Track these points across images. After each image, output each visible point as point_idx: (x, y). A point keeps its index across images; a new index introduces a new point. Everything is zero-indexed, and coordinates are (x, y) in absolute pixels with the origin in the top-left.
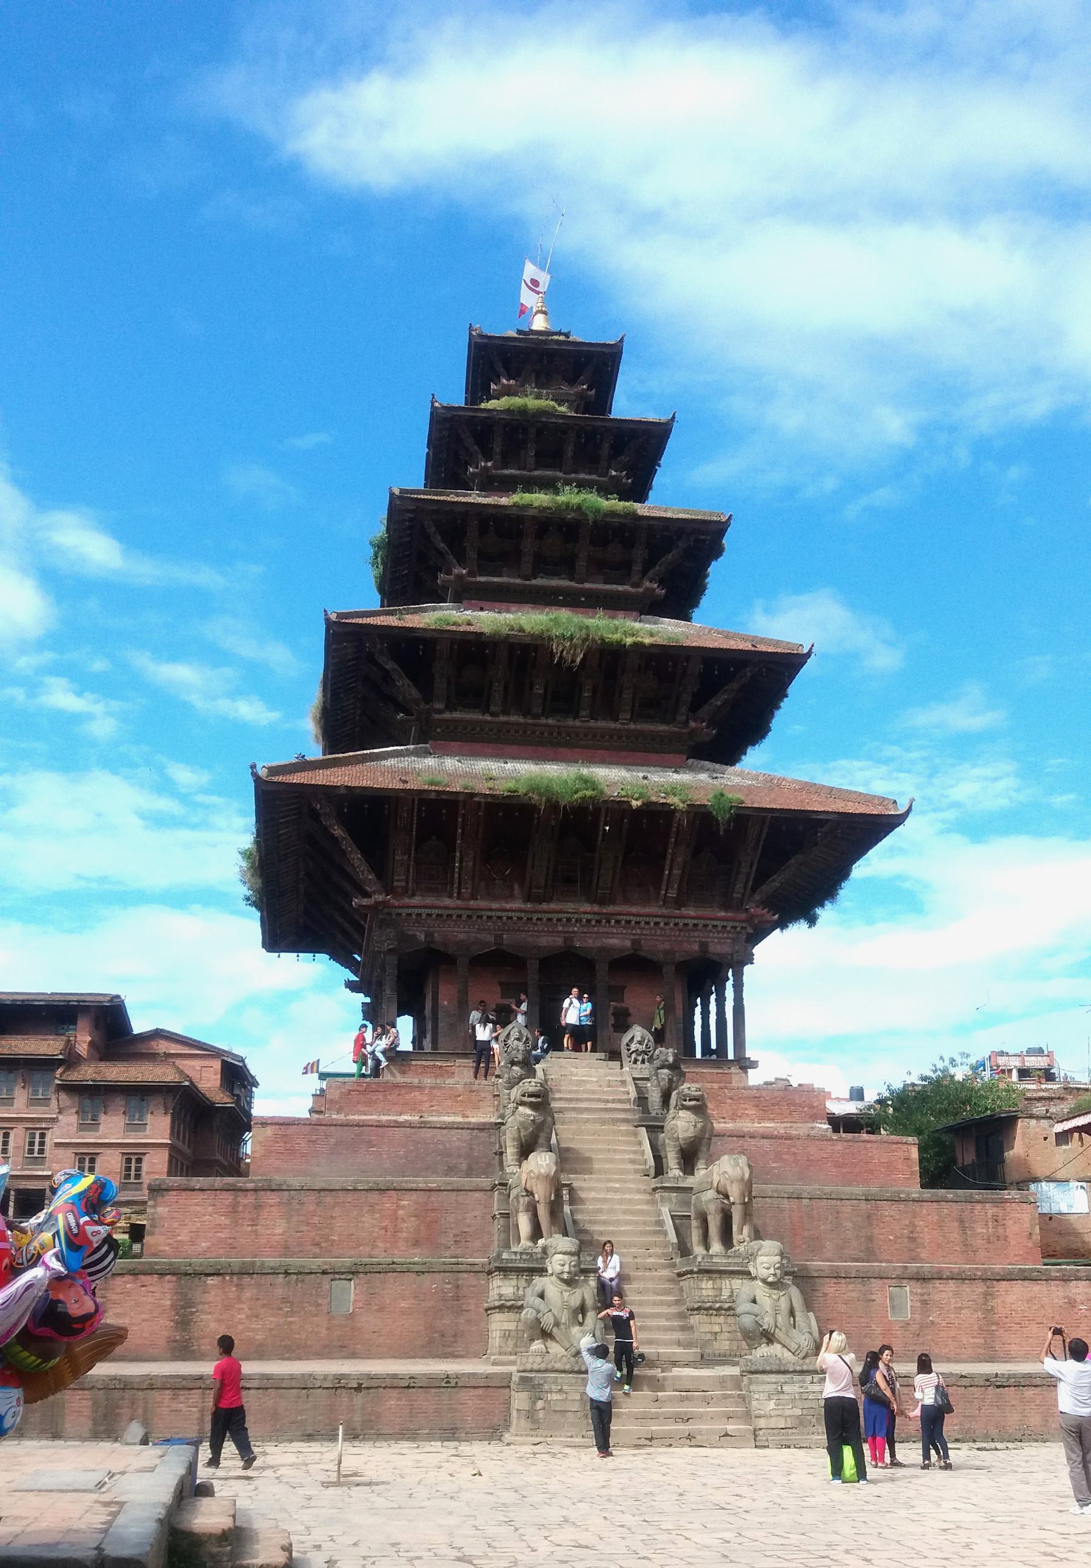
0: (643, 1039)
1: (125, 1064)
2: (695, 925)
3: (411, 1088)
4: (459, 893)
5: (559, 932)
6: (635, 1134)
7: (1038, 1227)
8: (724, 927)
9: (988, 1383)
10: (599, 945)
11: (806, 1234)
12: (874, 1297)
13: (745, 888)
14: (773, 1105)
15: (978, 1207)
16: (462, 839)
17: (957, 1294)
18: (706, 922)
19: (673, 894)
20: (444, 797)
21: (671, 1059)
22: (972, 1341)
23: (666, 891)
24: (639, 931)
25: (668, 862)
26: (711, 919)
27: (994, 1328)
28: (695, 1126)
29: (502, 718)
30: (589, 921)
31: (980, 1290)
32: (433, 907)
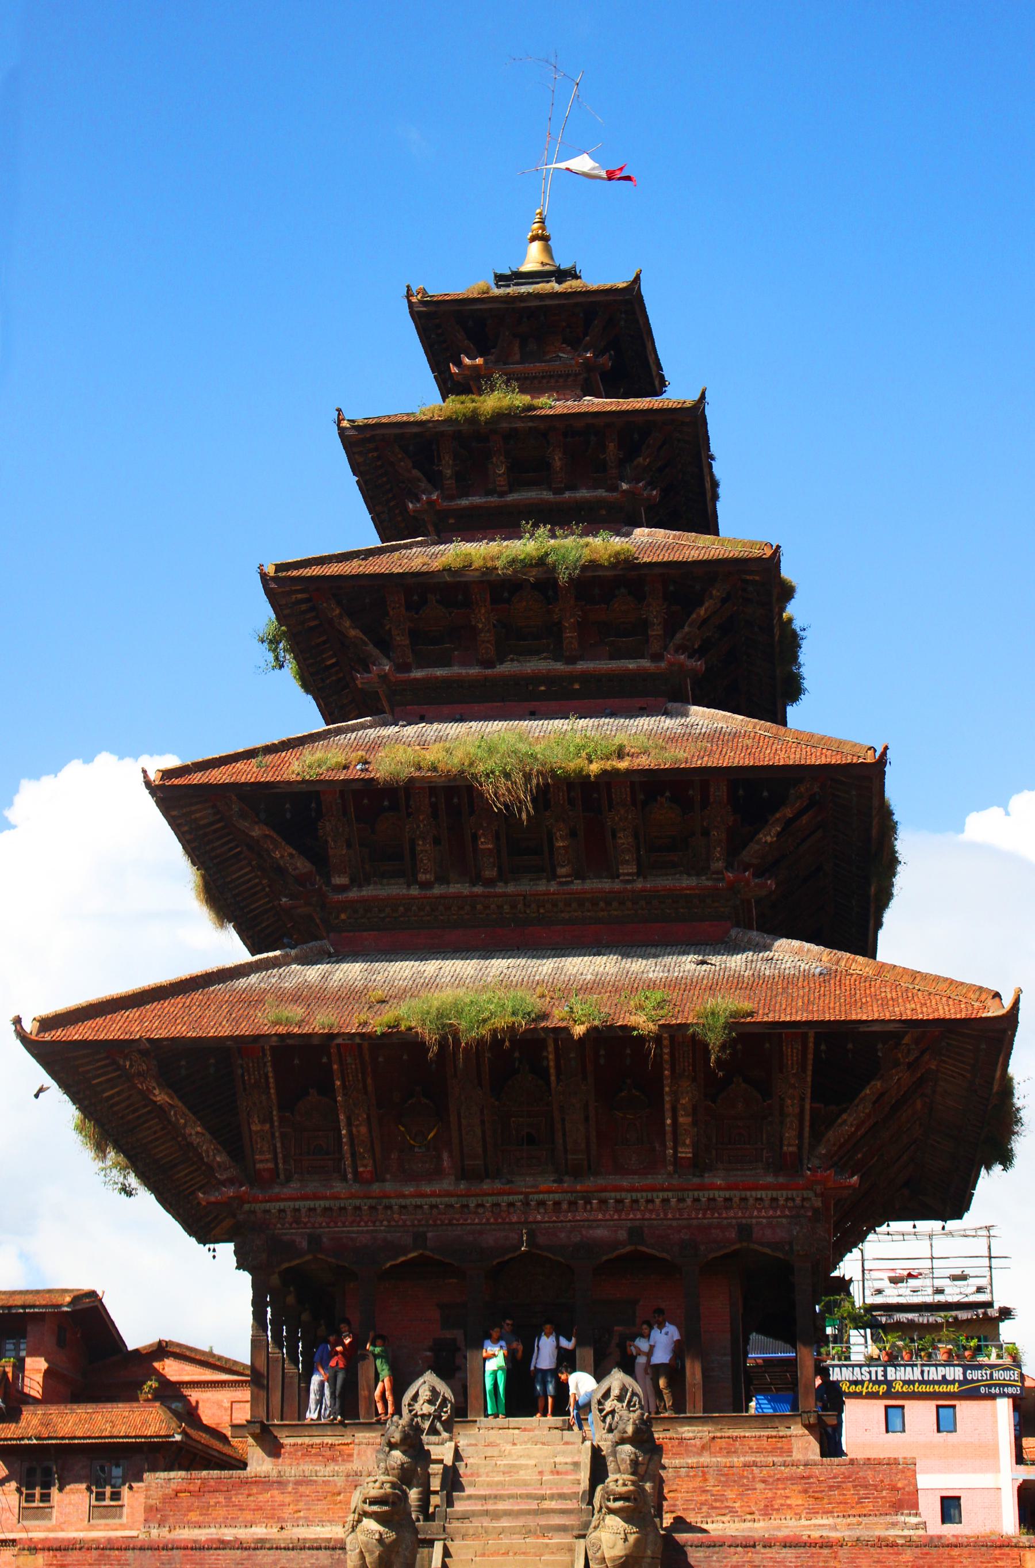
0: (624, 1389)
1: (90, 1408)
2: (726, 1200)
3: (263, 1483)
4: (356, 1173)
5: (511, 1223)
6: (571, 1550)
8: (774, 1200)
16: (344, 1095)
18: (743, 1194)
19: (686, 1152)
20: (290, 1042)
21: (630, 1429)
24: (639, 1216)
25: (667, 1106)
26: (750, 1189)
28: (626, 1540)
29: (437, 890)
30: (557, 1204)
32: (316, 1197)
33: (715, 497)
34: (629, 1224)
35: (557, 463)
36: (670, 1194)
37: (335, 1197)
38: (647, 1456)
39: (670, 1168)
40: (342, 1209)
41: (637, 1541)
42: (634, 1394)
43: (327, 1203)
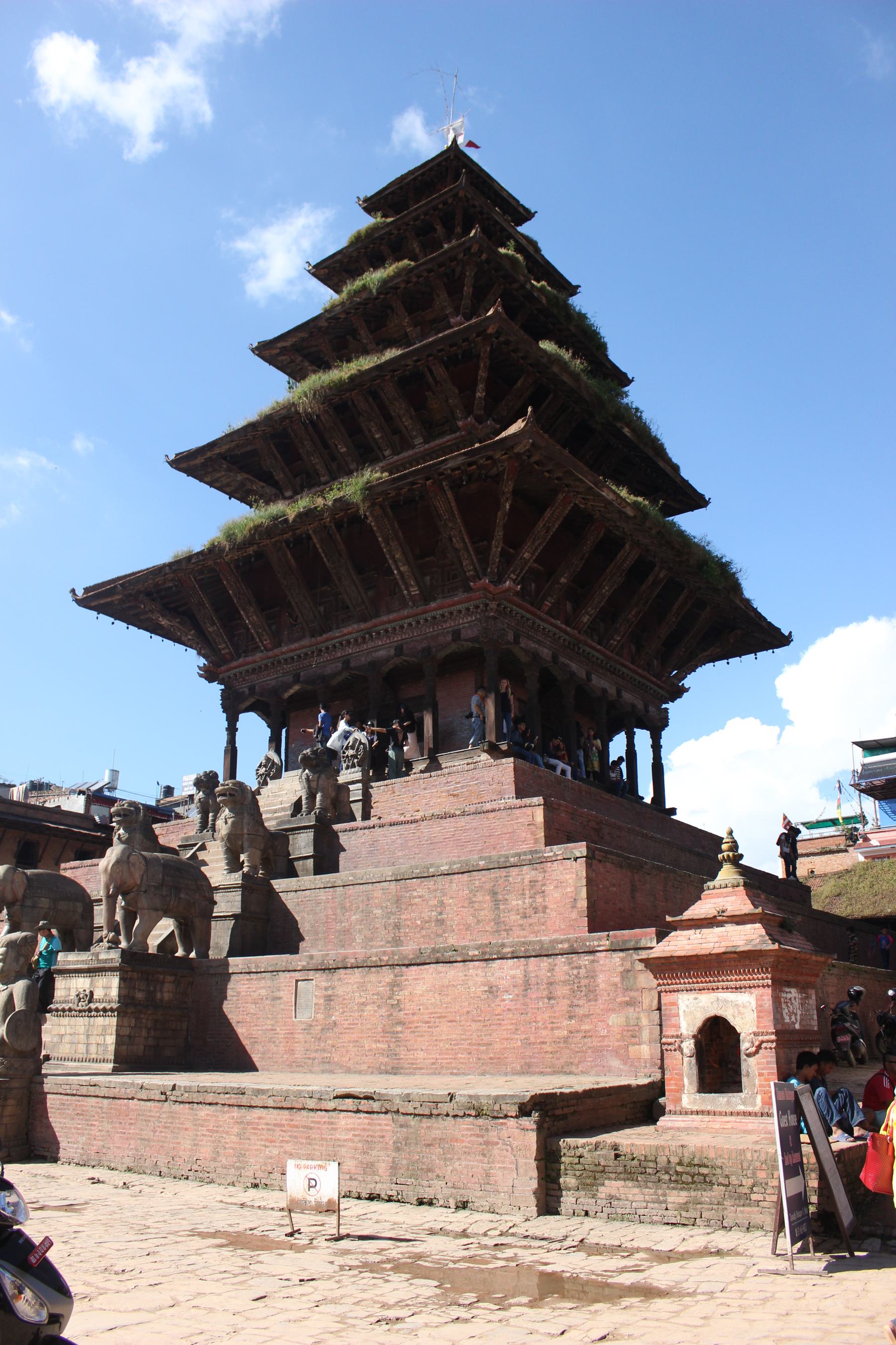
2: (443, 616)
4: (263, 645)
7: (584, 890)
8: (468, 609)
9: (163, 1097)
10: (369, 660)
11: (338, 927)
12: (281, 994)
13: (473, 563)
14: (462, 787)
15: (514, 871)
17: (362, 987)
19: (415, 591)
22: (374, 1046)
23: (407, 589)
27: (399, 1029)
28: (226, 823)
31: (387, 980)
33: (538, 250)
34: (395, 644)
35: (417, 250)
36: (411, 619)
37: (255, 662)
38: (316, 776)
39: (410, 603)
40: (260, 667)
41: (233, 823)
42: (361, 743)
43: (253, 665)
